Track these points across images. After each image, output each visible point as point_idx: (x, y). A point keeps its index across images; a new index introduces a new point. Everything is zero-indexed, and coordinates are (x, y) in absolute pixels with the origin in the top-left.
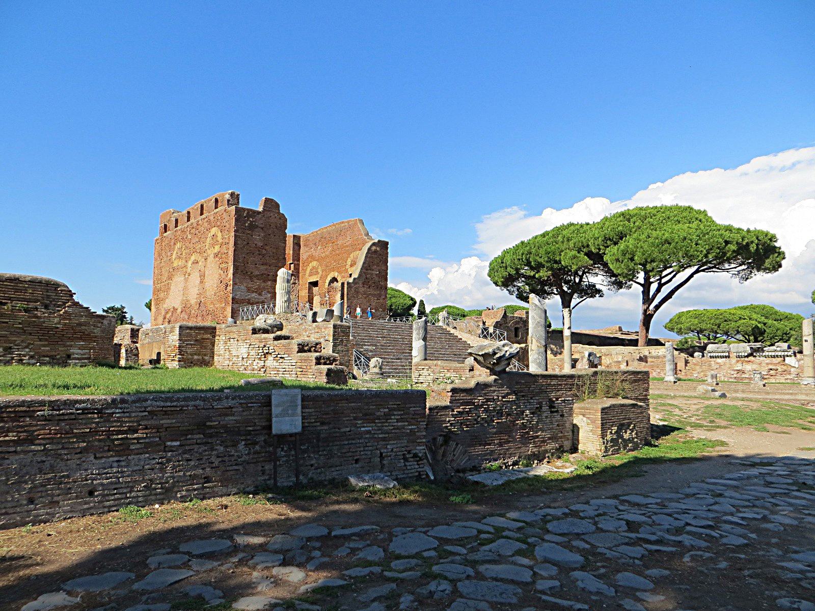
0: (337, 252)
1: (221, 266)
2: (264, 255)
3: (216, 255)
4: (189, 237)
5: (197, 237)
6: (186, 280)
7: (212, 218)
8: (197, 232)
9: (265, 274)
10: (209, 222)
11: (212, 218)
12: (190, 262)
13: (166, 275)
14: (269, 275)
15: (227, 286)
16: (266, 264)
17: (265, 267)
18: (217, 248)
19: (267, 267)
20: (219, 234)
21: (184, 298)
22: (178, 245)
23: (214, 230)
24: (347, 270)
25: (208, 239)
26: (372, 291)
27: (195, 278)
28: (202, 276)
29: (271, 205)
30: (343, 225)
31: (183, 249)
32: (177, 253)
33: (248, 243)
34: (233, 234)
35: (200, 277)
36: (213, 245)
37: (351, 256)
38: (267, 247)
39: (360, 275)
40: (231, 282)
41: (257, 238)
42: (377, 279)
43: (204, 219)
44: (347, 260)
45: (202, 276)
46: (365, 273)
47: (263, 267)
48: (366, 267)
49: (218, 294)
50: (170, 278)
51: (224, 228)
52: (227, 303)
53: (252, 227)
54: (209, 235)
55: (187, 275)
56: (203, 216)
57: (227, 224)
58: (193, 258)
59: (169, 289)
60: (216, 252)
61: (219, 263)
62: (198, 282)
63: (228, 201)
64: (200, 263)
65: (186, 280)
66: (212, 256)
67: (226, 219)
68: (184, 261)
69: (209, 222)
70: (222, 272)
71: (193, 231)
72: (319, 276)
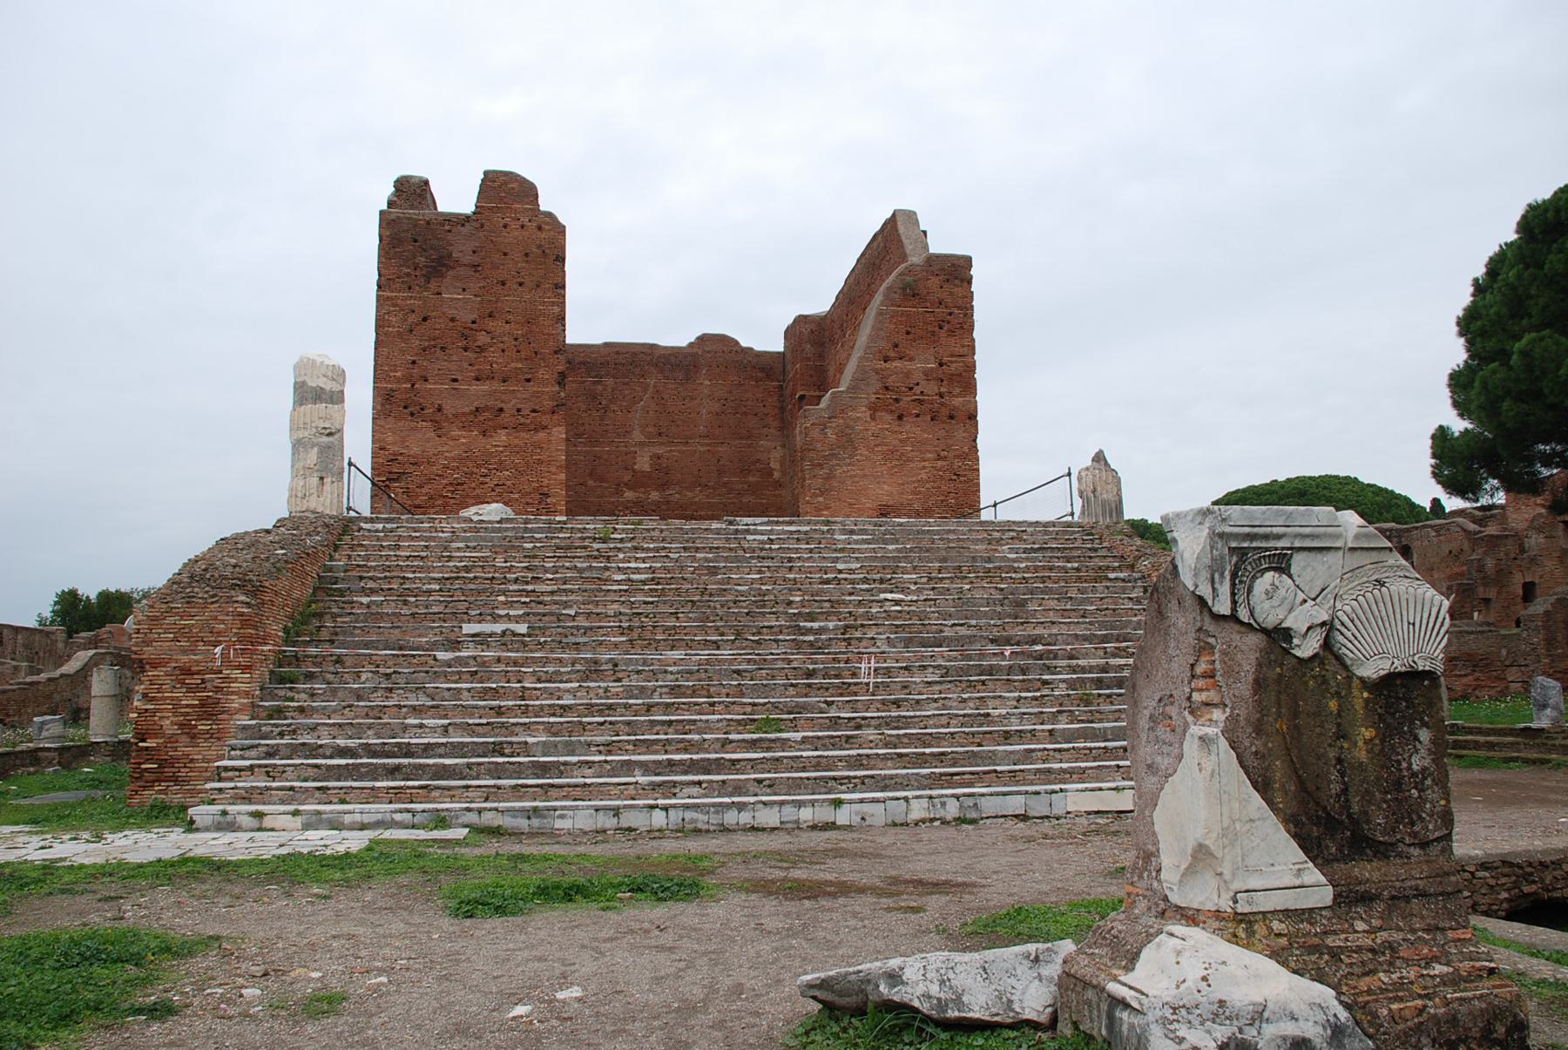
2: (481, 349)
9: (486, 408)
14: (501, 410)
17: (485, 387)
19: (497, 386)
26: (910, 428)
29: (506, 193)
33: (425, 319)
38: (491, 324)
41: (457, 299)
42: (931, 388)
47: (477, 388)
53: (439, 265)
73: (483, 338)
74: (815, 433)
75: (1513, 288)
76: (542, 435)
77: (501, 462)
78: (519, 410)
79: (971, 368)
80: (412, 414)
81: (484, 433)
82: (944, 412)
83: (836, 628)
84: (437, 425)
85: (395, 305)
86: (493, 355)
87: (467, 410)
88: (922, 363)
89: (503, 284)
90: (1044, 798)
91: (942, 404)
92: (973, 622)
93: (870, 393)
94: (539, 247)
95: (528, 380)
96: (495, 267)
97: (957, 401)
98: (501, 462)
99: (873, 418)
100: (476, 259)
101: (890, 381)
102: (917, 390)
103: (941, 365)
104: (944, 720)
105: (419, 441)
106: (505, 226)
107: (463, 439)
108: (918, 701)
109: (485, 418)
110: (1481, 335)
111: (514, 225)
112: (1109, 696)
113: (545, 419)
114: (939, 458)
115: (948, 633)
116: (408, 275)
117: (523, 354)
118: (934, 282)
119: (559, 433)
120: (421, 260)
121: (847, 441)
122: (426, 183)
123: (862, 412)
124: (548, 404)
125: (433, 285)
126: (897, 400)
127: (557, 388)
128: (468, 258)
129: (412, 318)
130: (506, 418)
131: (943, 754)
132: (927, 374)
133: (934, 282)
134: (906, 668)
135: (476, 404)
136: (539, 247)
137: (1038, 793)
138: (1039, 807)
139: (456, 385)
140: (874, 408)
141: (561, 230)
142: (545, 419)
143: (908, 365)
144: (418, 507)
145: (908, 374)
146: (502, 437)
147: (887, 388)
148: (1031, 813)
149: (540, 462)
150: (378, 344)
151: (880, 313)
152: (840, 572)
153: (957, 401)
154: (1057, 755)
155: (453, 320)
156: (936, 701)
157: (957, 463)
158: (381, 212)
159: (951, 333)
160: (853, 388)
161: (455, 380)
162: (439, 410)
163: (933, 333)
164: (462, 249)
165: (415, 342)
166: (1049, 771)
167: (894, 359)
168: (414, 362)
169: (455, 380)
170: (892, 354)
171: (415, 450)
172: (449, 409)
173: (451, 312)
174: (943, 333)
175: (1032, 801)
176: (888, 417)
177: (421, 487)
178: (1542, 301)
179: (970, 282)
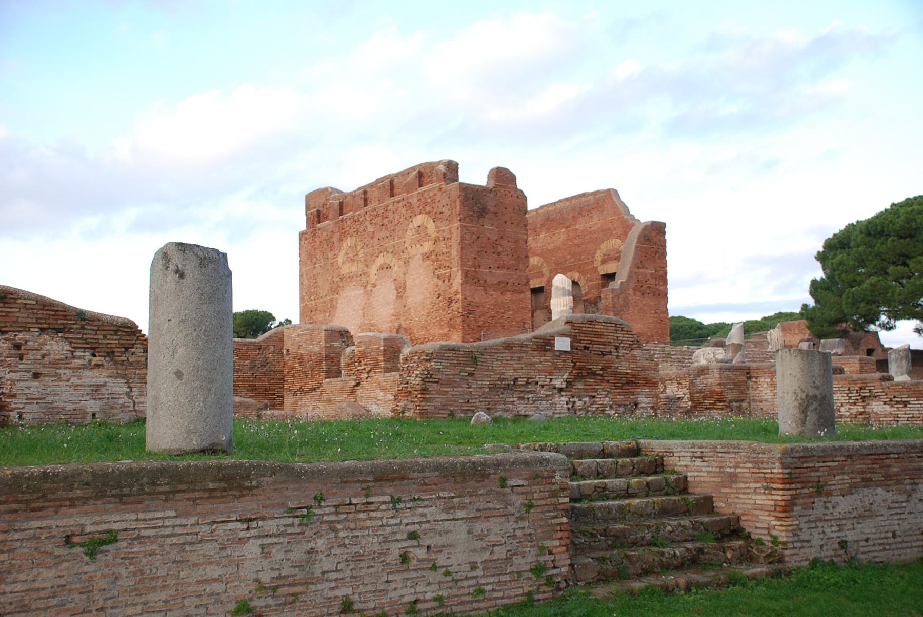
0: (576, 241)
1: (437, 272)
2: (499, 254)
3: (426, 257)
4: (371, 229)
5: (387, 229)
6: (368, 294)
7: (414, 201)
8: (385, 221)
10: (409, 206)
11: (414, 201)
12: (374, 269)
13: (327, 287)
15: (450, 301)
18: (427, 246)
20: (431, 226)
21: (366, 322)
22: (349, 242)
23: (419, 220)
24: (595, 270)
25: (409, 233)
27: (385, 292)
28: (401, 290)
30: (583, 199)
31: (359, 248)
32: (347, 254)
34: (458, 224)
35: (397, 289)
36: (420, 241)
37: (603, 246)
38: (503, 242)
39: (630, 277)
40: (459, 296)
42: (652, 281)
43: (399, 202)
44: (595, 253)
45: (401, 290)
47: (499, 272)
48: (639, 264)
49: (435, 314)
50: (336, 290)
51: (438, 216)
52: (451, 325)
53: (482, 213)
54: (411, 226)
55: (369, 288)
56: (396, 198)
57: (445, 210)
58: (380, 261)
59: (334, 307)
60: (425, 251)
61: (432, 267)
62: (392, 295)
64: (396, 269)
65: (368, 294)
66: (419, 257)
67: (444, 202)
68: (361, 266)
69: (409, 206)
70: (440, 283)
71: (378, 220)
72: (545, 279)
73: (500, 249)
74: (616, 300)
75: (860, 255)
76: (522, 295)
79: (666, 273)
82: (657, 293)
84: (485, 290)
86: (504, 257)
93: (633, 284)
96: (503, 215)
97: (661, 288)
101: (641, 278)
105: (479, 296)
110: (846, 272)
118: (654, 233)
120: (476, 209)
122: (458, 164)
123: (631, 292)
129: (474, 237)
130: (510, 287)
132: (652, 275)
133: (654, 233)
140: (635, 290)
141: (525, 198)
145: (646, 275)
146: (508, 295)
151: (636, 247)
153: (661, 288)
160: (628, 281)
164: (491, 205)
171: (477, 300)
172: (489, 282)
173: (488, 235)
176: (639, 294)
178: (874, 262)
179: (664, 233)
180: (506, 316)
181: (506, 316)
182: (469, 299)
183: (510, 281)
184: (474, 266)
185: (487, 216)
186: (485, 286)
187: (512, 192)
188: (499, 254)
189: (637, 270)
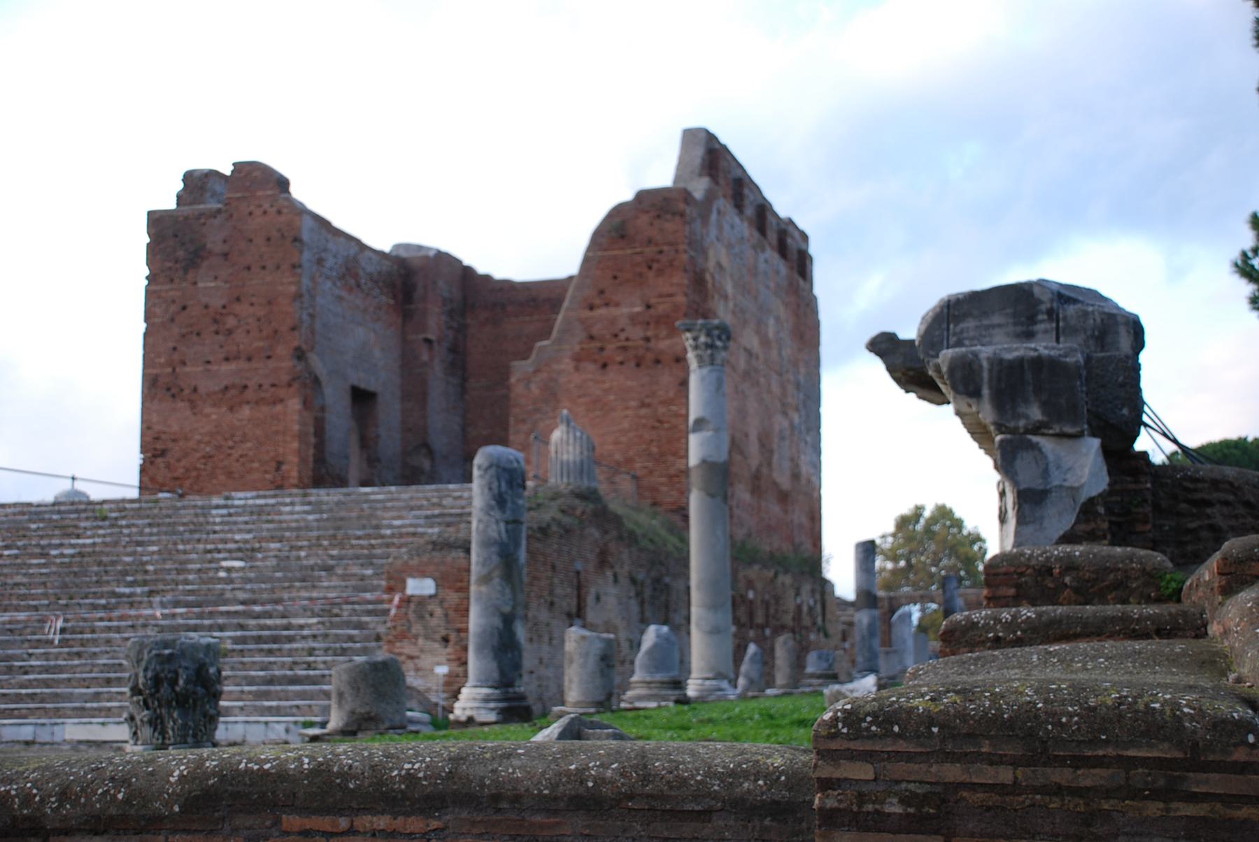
2: (230, 332)
9: (234, 386)
14: (246, 387)
16: (237, 358)
17: (232, 366)
19: (243, 364)
26: (614, 378)
33: (184, 308)
38: (237, 308)
41: (209, 286)
42: (636, 333)
46: (582, 321)
47: (226, 368)
63: (180, 198)
73: (231, 322)
76: (279, 408)
77: (244, 435)
78: (260, 386)
80: (173, 396)
81: (231, 409)
82: (650, 357)
83: (143, 594)
85: (159, 297)
87: (217, 388)
88: (629, 307)
89: (249, 268)
90: (48, 729)
91: (648, 349)
92: (248, 586)
94: (279, 230)
95: (269, 357)
98: (244, 435)
99: (577, 369)
100: (226, 248)
101: (595, 331)
102: (622, 336)
103: (648, 307)
104: (88, 668)
105: (178, 418)
106: (251, 214)
107: (215, 414)
108: (95, 654)
109: (233, 395)
111: (258, 212)
112: (242, 651)
113: (282, 393)
114: (643, 405)
115: (228, 595)
116: (170, 268)
117: (265, 333)
118: (644, 220)
119: (295, 404)
120: (181, 253)
121: (551, 395)
123: (567, 364)
124: (285, 378)
125: (190, 276)
126: (602, 349)
127: (295, 362)
128: (219, 247)
129: (173, 308)
130: (249, 394)
131: (35, 694)
132: (633, 319)
133: (644, 220)
134: (133, 626)
135: (225, 383)
136: (279, 230)
137: (43, 725)
138: (44, 736)
139: (209, 367)
140: (578, 359)
142: (282, 393)
143: (613, 311)
144: (176, 479)
145: (613, 321)
146: (246, 411)
147: (592, 338)
148: (39, 740)
149: (277, 432)
150: (146, 335)
152: (237, 542)
153: (664, 345)
154: (119, 697)
155: (206, 307)
156: (107, 652)
157: (662, 410)
158: (150, 214)
159: (660, 272)
161: (208, 362)
162: (195, 390)
163: (641, 275)
165: (176, 330)
166: (83, 709)
167: (599, 307)
168: (175, 349)
169: (208, 362)
170: (597, 301)
174: (651, 274)
175: (40, 730)
176: (591, 367)
177: (179, 460)
180: (236, 453)
181: (236, 453)
182: (157, 428)
183: (252, 384)
184: (170, 363)
185: (205, 264)
186: (193, 399)
187: (266, 206)
188: (230, 332)
189: (587, 313)
